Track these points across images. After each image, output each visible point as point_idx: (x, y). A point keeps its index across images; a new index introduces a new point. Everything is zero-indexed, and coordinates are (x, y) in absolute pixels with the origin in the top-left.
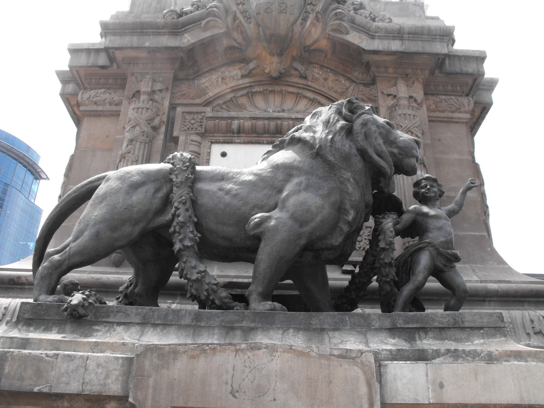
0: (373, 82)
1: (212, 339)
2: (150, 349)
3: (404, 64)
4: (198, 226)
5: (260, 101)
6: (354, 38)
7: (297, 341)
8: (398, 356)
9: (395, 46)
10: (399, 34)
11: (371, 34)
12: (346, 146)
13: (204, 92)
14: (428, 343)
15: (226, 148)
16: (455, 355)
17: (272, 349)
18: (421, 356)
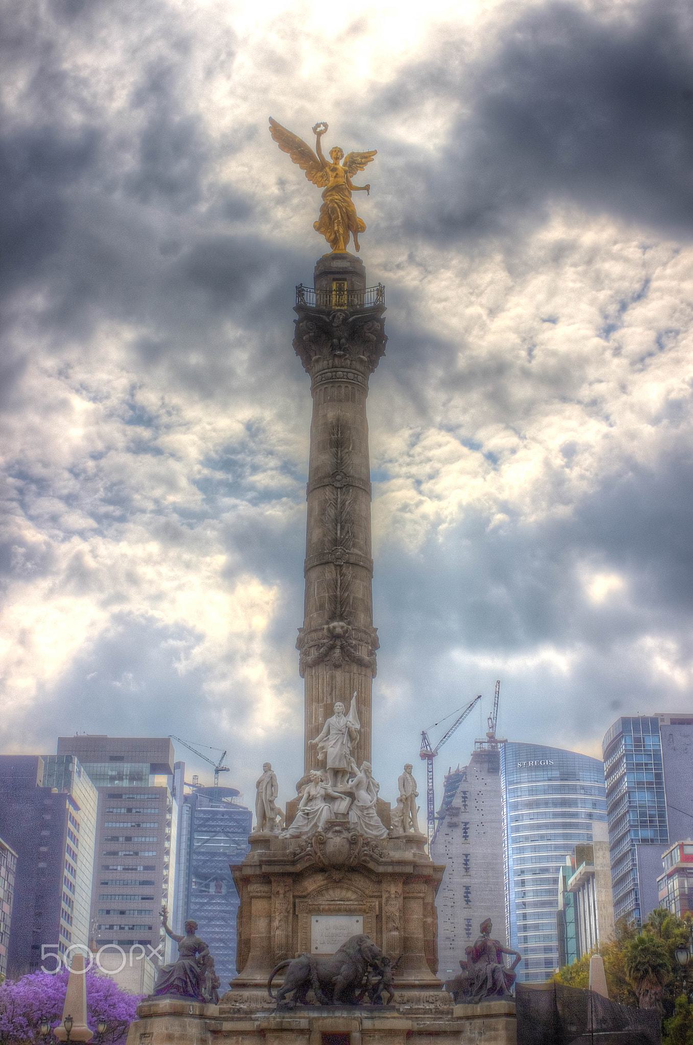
0: (379, 882)
1: (325, 1015)
2: (314, 1018)
3: (394, 876)
4: (319, 980)
5: (331, 892)
6: (371, 865)
7: (345, 1015)
8: (366, 1018)
9: (390, 869)
10: (392, 863)
11: (378, 863)
12: (359, 956)
13: (307, 889)
14: (376, 1014)
15: (319, 918)
16: (380, 1018)
17: (339, 1018)
18: (372, 1018)
